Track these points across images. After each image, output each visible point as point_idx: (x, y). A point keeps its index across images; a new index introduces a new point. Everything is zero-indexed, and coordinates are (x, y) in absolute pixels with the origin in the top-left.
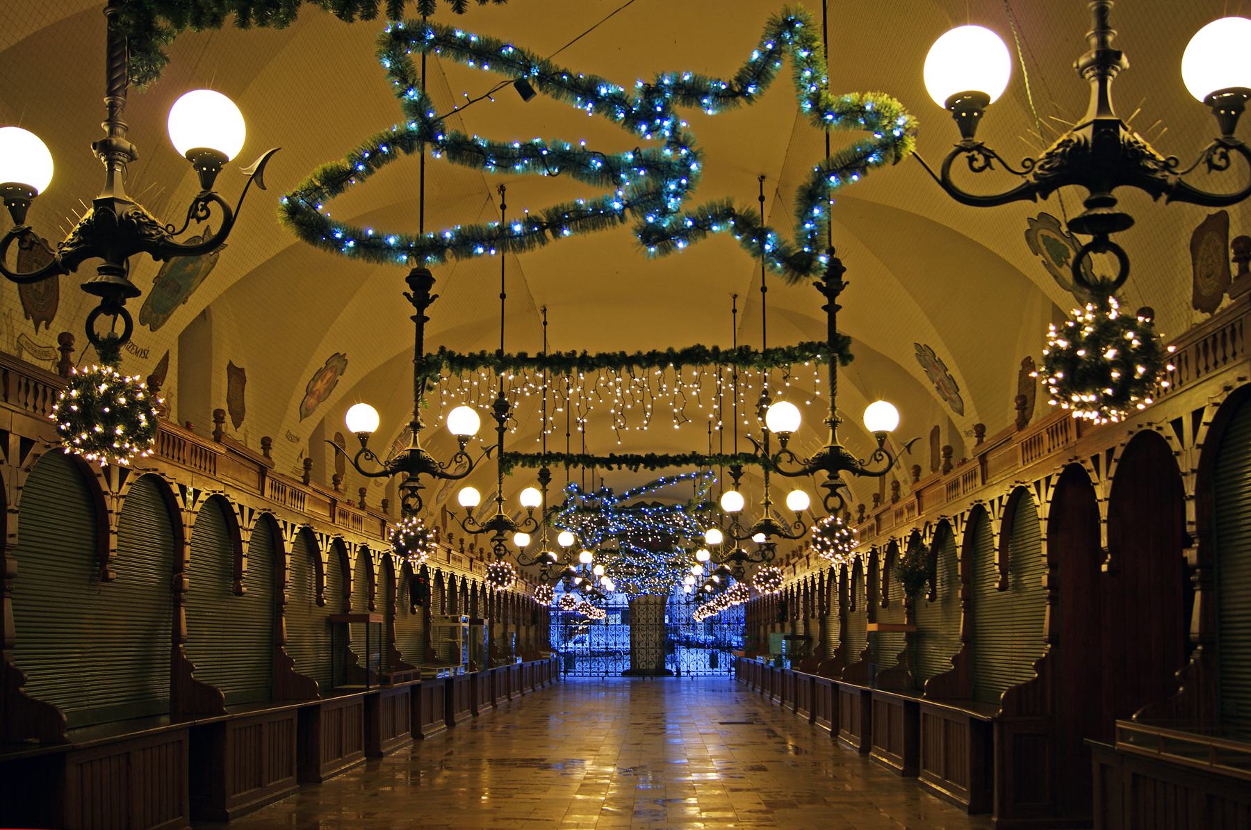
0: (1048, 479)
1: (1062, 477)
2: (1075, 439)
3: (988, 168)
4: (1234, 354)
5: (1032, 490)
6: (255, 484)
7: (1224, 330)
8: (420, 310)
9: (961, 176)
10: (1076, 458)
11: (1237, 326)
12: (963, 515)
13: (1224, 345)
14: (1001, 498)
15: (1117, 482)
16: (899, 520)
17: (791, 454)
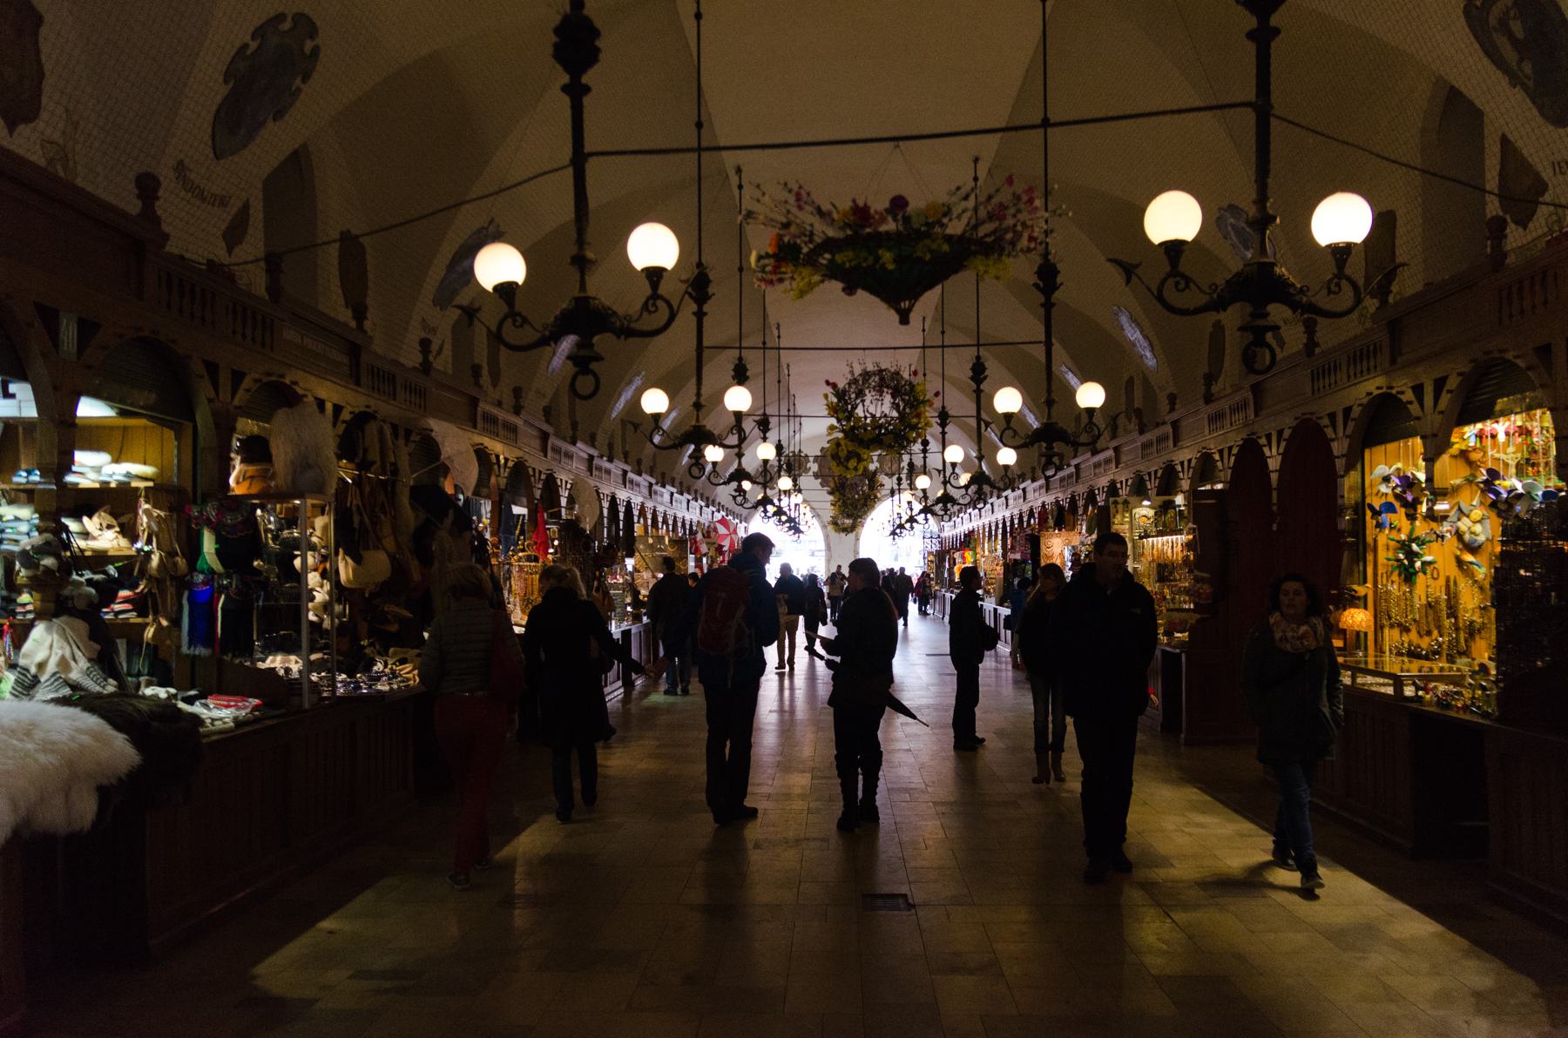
0: (1230, 448)
1: (1241, 447)
2: (1252, 417)
3: (1187, 291)
4: (1375, 367)
5: (1217, 457)
6: (538, 447)
7: (1368, 347)
8: (700, 306)
9: (1170, 294)
10: (1253, 434)
11: (1378, 345)
12: (1156, 472)
13: (1368, 359)
14: (1190, 461)
15: (1285, 455)
16: (1097, 471)
17: (1015, 431)
